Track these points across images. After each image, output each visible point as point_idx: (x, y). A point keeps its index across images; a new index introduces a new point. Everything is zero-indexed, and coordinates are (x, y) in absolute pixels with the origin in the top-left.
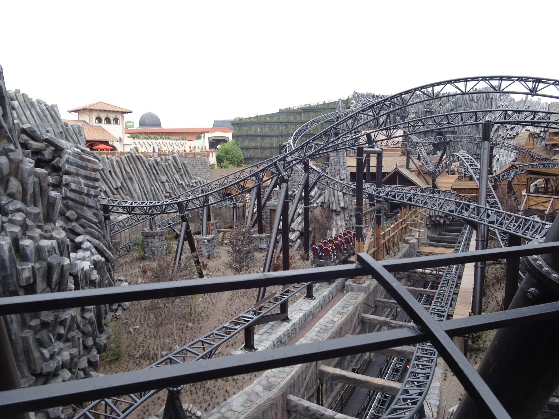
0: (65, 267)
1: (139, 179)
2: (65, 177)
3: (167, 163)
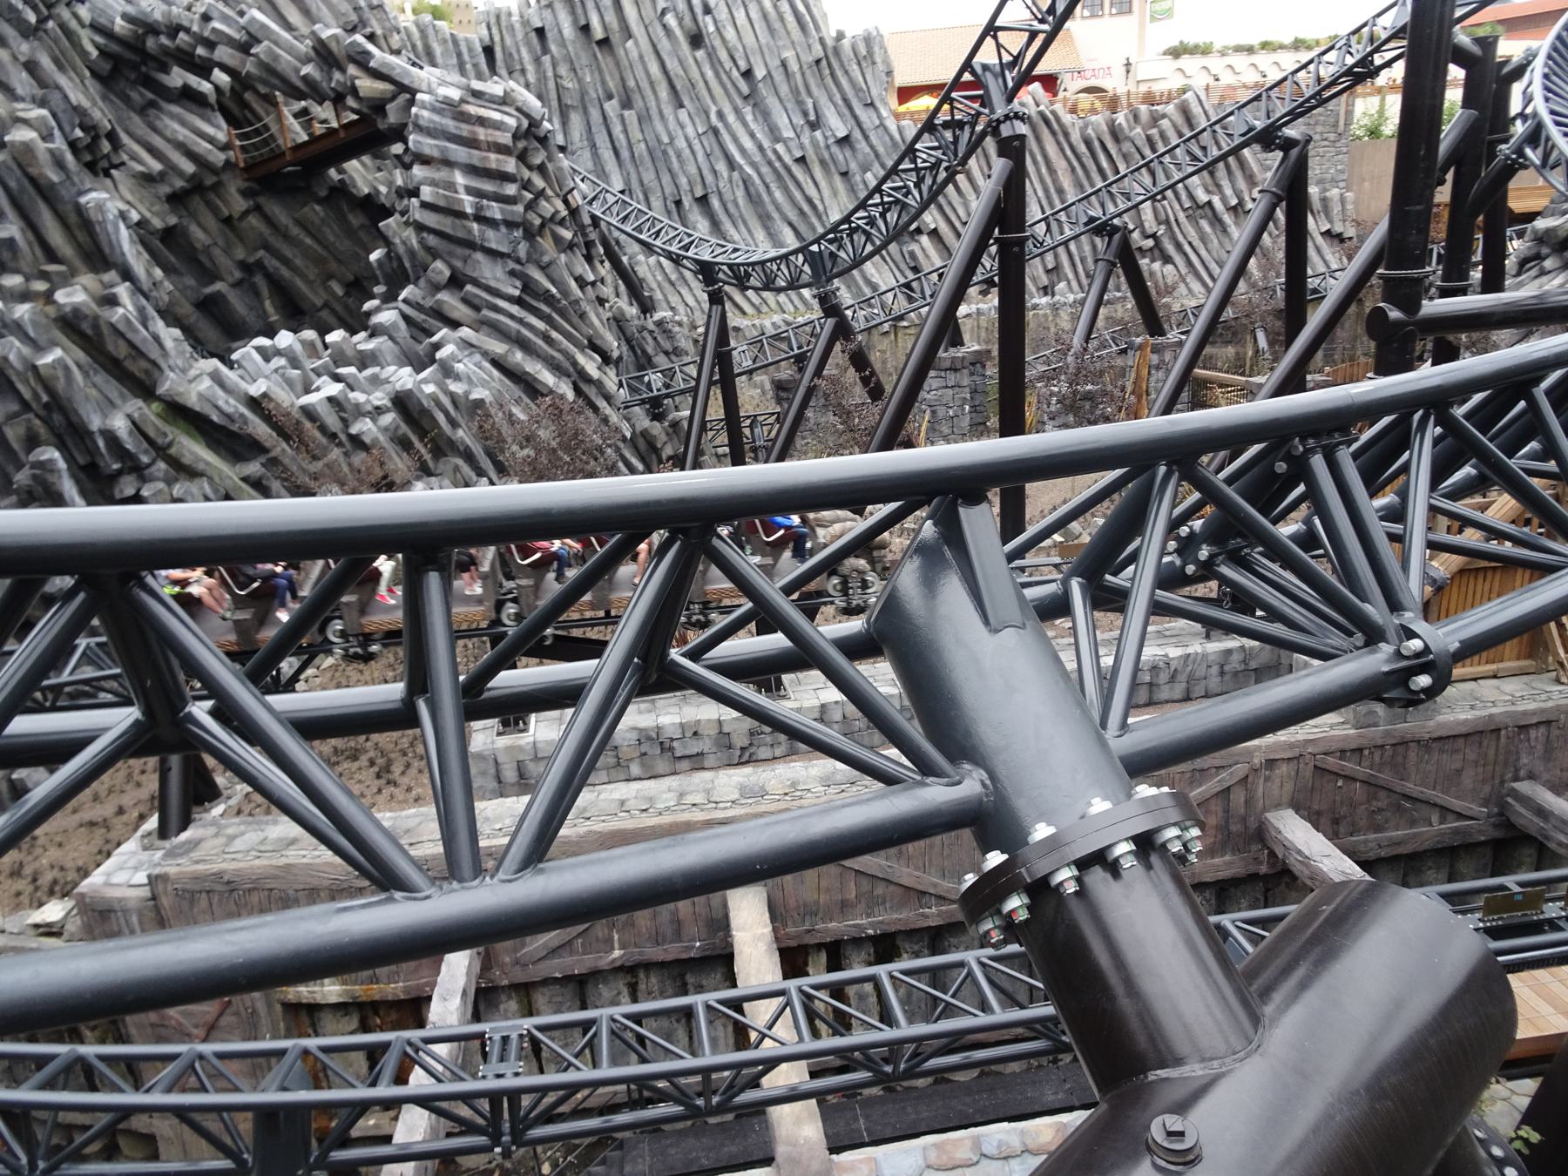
0: (42, 371)
1: (1046, 190)
2: (418, 171)
3: (1154, 131)
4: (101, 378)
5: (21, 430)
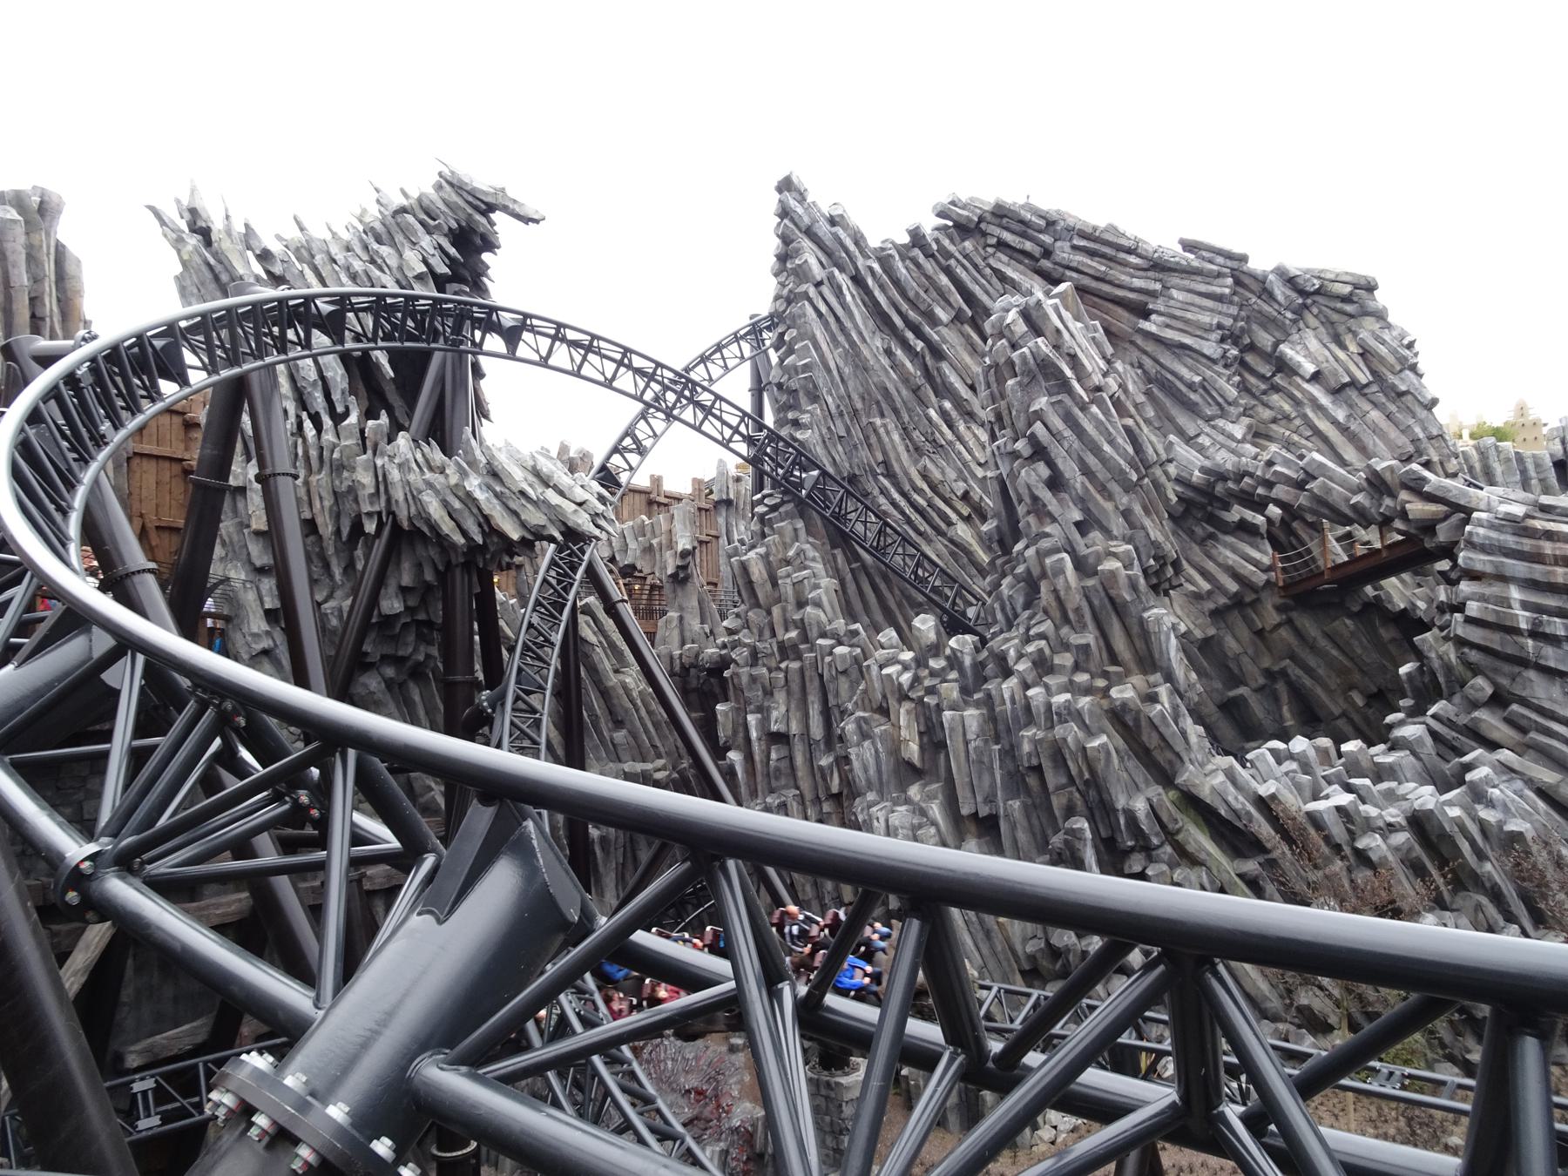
0: (1089, 752)
2: (1465, 587)
4: (1132, 764)
5: (1064, 801)
